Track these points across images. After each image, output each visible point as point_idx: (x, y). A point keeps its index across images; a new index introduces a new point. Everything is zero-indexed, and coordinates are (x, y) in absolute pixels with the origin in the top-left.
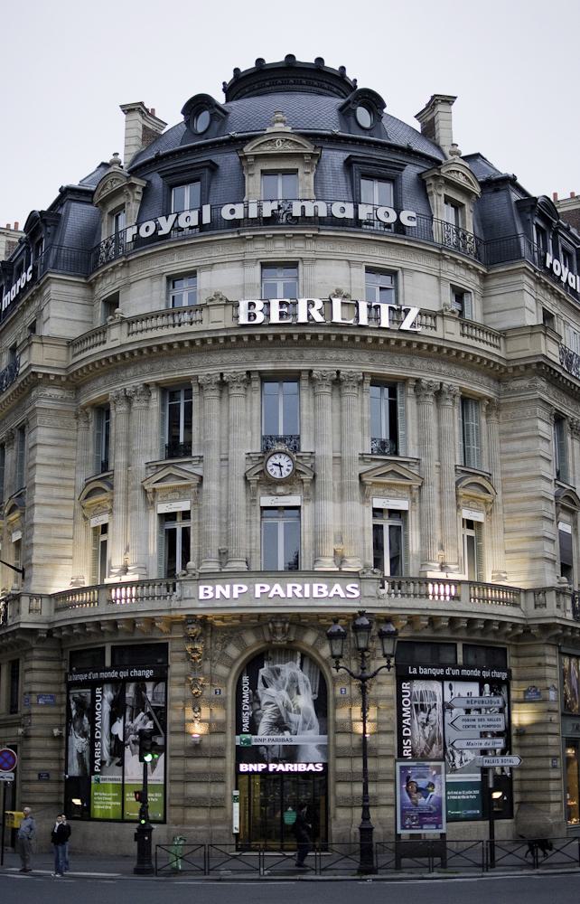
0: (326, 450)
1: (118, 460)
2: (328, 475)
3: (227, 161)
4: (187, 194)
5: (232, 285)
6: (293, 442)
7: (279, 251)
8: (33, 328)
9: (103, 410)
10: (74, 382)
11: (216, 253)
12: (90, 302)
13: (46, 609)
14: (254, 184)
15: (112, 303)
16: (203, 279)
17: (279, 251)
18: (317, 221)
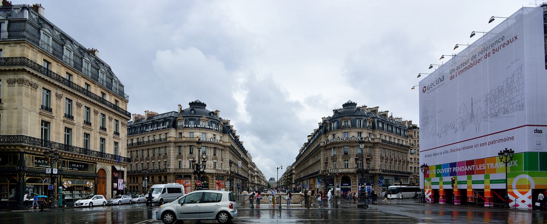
0: (209, 155)
1: (183, 154)
2: (209, 158)
3: (197, 118)
4: (192, 122)
5: (197, 134)
6: (205, 153)
7: (204, 131)
8: (166, 134)
9: (180, 147)
10: (175, 143)
11: (196, 131)
12: (176, 132)
13: (173, 170)
14: (201, 123)
15: (181, 133)
16: (195, 133)
17: (204, 131)
18: (208, 129)
